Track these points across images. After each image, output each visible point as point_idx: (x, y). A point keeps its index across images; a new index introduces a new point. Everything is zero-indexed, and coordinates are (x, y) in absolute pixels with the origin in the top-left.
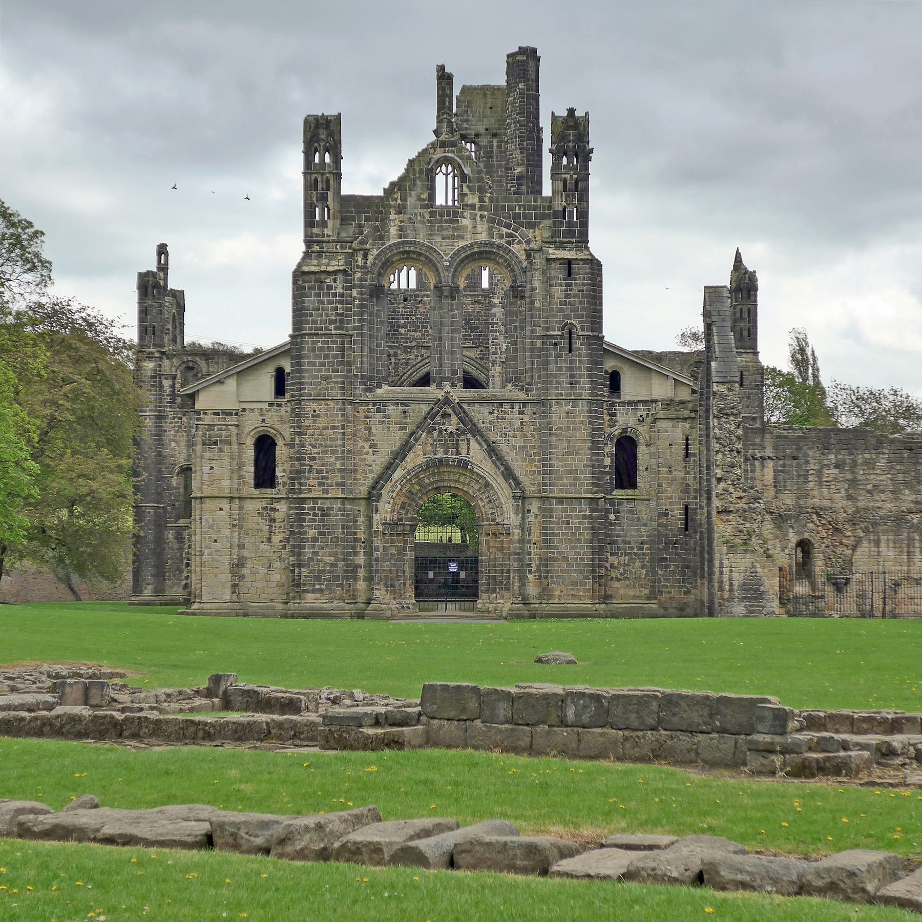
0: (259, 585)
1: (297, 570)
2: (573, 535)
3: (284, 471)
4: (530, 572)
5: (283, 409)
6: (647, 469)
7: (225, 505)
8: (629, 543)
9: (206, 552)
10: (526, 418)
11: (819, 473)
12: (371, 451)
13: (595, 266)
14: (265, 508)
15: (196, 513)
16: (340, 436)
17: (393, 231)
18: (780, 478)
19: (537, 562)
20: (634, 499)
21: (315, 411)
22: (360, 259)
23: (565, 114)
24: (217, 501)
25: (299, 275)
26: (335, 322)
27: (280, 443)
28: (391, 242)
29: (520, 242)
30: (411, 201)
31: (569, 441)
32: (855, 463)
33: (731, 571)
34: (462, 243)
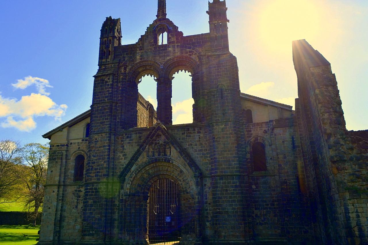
2: (230, 197)
4: (208, 221)
6: (271, 158)
8: (265, 202)
10: (202, 135)
14: (76, 191)
17: (138, 57)
19: (212, 215)
20: (266, 176)
22: (122, 70)
26: (108, 97)
28: (137, 62)
29: (195, 54)
30: (145, 44)
31: (224, 144)
33: (358, 216)
34: (168, 58)
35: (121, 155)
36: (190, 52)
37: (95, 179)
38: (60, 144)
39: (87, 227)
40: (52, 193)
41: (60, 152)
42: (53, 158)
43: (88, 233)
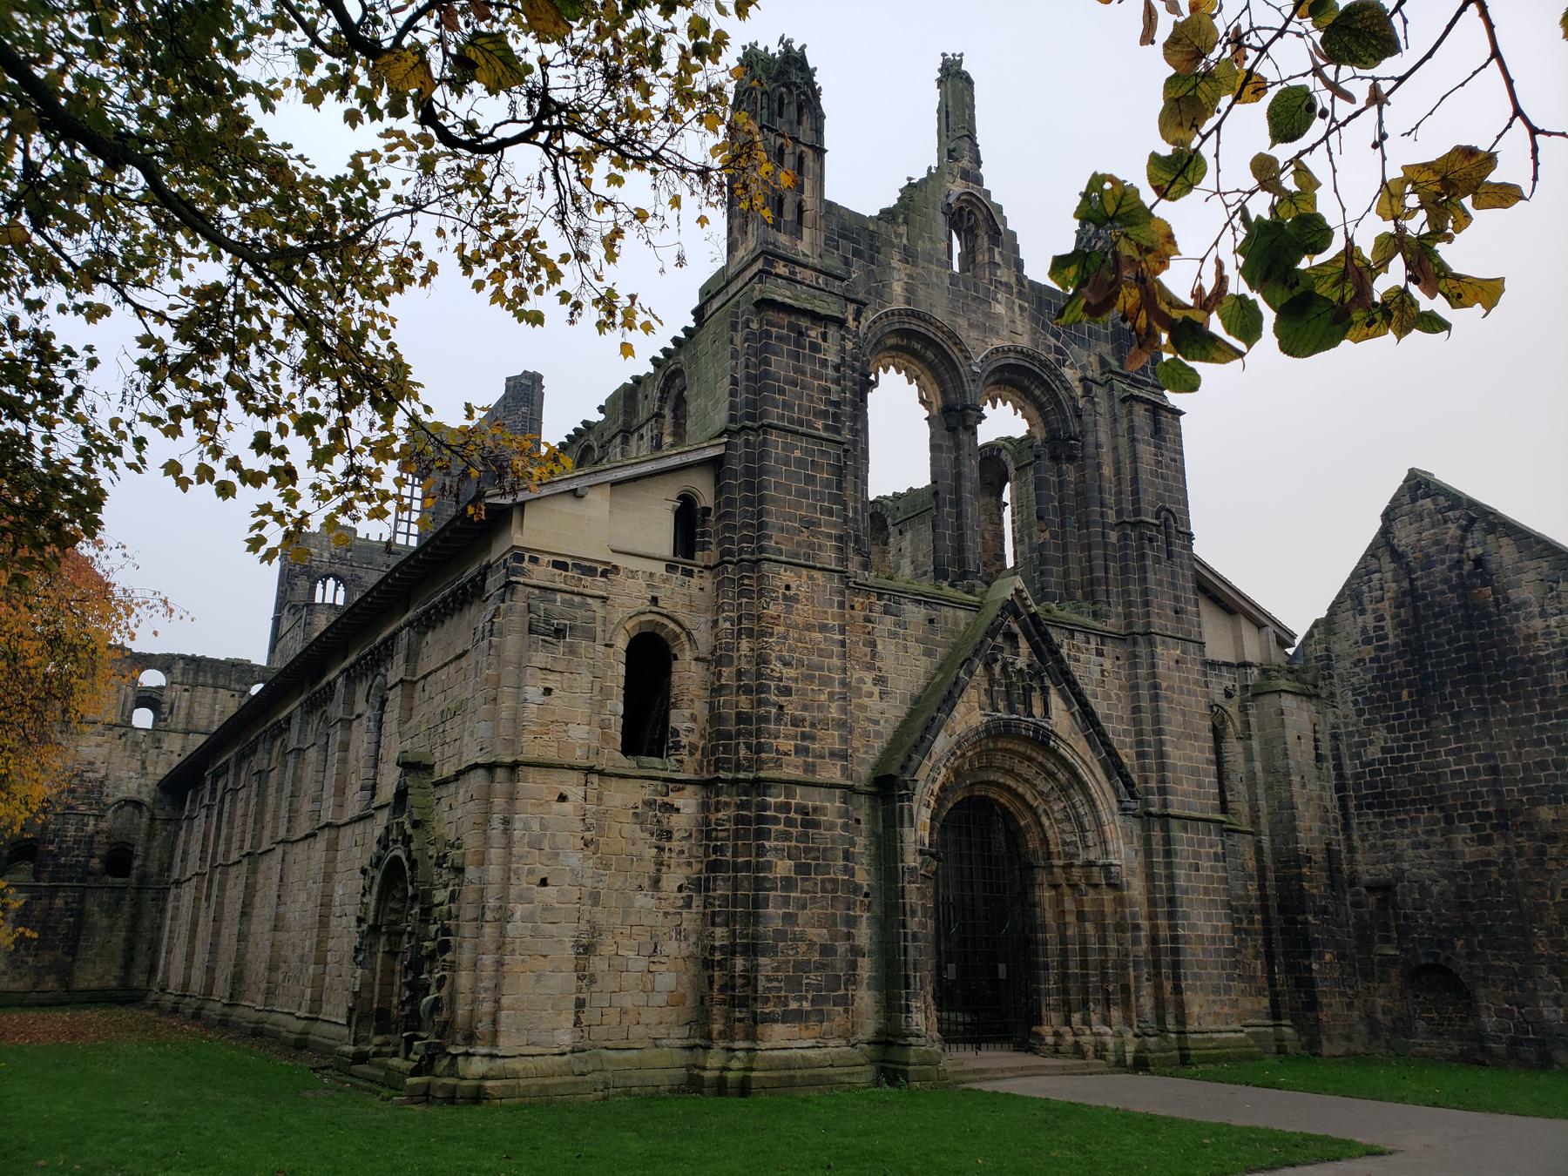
0: (627, 1002)
1: (739, 963)
3: (693, 718)
5: (695, 581)
7: (572, 785)
9: (519, 910)
10: (1108, 665)
12: (876, 690)
14: (649, 804)
16: (836, 649)
17: (898, 288)
21: (788, 588)
24: (557, 775)
26: (824, 414)
31: (1184, 715)
35: (868, 677)
37: (796, 767)
38: (570, 562)
39: (775, 984)
40: (557, 806)
41: (577, 599)
42: (547, 623)
43: (779, 1010)
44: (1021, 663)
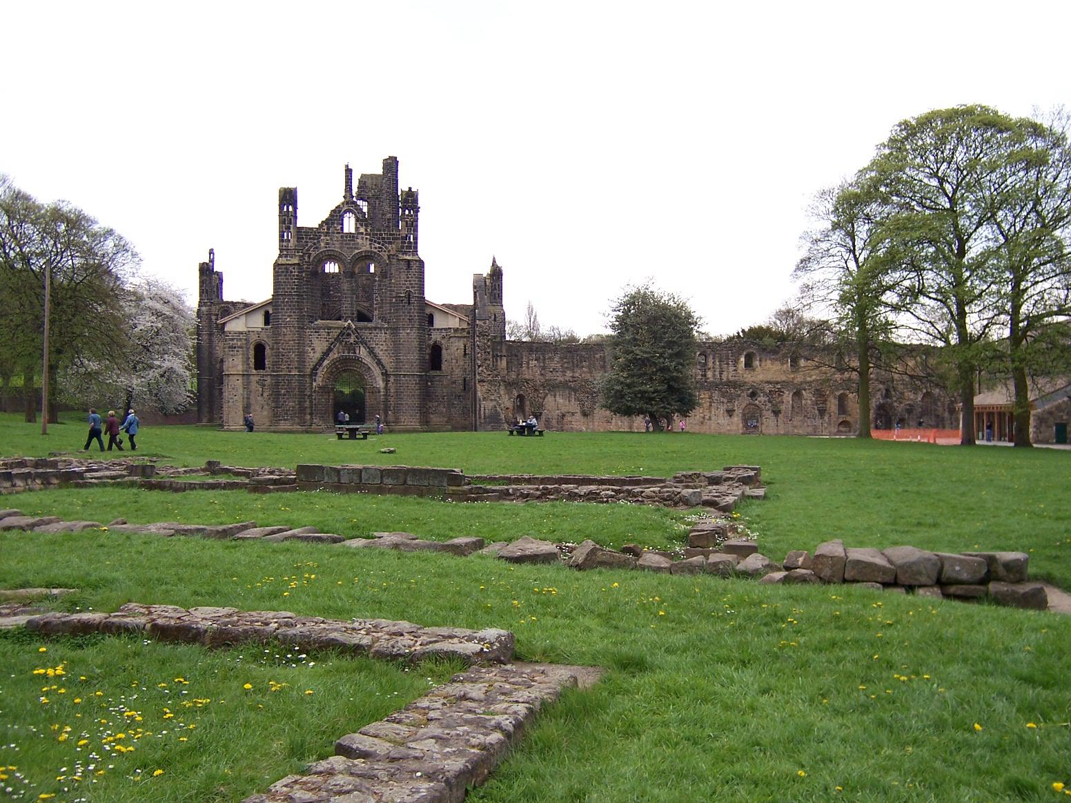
11: (528, 363)
13: (421, 263)
15: (225, 382)
18: (510, 365)
23: (407, 190)
25: (276, 265)
27: (267, 348)
32: (544, 359)
34: (357, 251)
36: (380, 248)
44: (352, 341)
